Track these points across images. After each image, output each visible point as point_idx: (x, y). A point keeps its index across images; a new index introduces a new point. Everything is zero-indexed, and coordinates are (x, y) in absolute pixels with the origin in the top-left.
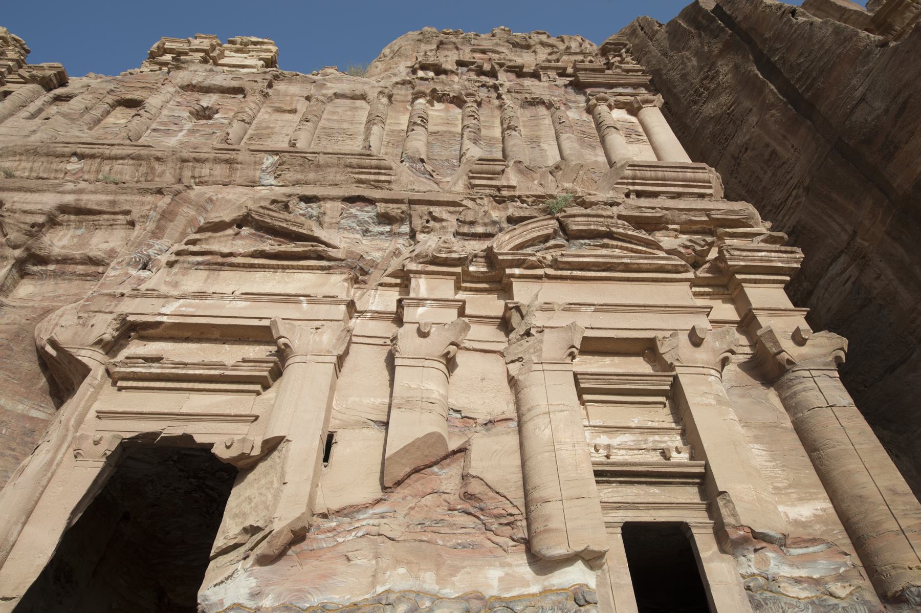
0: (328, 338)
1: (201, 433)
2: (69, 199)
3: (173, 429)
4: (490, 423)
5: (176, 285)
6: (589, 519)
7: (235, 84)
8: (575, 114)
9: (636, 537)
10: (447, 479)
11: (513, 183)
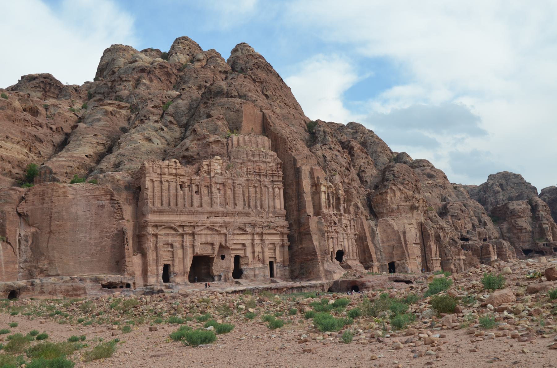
6: (267, 262)
8: (271, 190)
9: (270, 262)
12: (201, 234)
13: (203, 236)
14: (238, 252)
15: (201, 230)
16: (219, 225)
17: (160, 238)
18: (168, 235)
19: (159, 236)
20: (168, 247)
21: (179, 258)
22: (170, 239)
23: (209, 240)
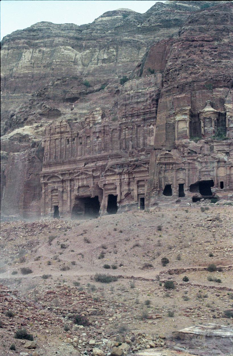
0: (118, 184)
1: (113, 194)
2: (93, 169)
3: (111, 194)
4: (132, 190)
5: (106, 179)
7: (99, 131)
10: (130, 195)
11: (134, 155)
12: (78, 179)
13: (80, 181)
14: (112, 191)
15: (78, 176)
16: (91, 169)
17: (49, 186)
18: (54, 182)
19: (49, 184)
20: (57, 193)
21: (63, 200)
22: (56, 186)
23: (85, 183)
